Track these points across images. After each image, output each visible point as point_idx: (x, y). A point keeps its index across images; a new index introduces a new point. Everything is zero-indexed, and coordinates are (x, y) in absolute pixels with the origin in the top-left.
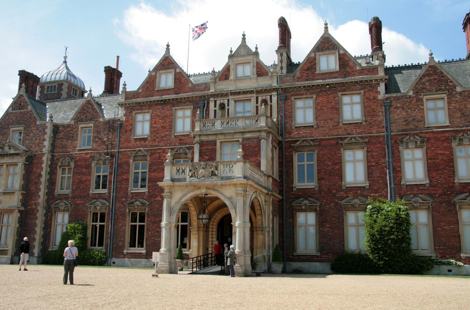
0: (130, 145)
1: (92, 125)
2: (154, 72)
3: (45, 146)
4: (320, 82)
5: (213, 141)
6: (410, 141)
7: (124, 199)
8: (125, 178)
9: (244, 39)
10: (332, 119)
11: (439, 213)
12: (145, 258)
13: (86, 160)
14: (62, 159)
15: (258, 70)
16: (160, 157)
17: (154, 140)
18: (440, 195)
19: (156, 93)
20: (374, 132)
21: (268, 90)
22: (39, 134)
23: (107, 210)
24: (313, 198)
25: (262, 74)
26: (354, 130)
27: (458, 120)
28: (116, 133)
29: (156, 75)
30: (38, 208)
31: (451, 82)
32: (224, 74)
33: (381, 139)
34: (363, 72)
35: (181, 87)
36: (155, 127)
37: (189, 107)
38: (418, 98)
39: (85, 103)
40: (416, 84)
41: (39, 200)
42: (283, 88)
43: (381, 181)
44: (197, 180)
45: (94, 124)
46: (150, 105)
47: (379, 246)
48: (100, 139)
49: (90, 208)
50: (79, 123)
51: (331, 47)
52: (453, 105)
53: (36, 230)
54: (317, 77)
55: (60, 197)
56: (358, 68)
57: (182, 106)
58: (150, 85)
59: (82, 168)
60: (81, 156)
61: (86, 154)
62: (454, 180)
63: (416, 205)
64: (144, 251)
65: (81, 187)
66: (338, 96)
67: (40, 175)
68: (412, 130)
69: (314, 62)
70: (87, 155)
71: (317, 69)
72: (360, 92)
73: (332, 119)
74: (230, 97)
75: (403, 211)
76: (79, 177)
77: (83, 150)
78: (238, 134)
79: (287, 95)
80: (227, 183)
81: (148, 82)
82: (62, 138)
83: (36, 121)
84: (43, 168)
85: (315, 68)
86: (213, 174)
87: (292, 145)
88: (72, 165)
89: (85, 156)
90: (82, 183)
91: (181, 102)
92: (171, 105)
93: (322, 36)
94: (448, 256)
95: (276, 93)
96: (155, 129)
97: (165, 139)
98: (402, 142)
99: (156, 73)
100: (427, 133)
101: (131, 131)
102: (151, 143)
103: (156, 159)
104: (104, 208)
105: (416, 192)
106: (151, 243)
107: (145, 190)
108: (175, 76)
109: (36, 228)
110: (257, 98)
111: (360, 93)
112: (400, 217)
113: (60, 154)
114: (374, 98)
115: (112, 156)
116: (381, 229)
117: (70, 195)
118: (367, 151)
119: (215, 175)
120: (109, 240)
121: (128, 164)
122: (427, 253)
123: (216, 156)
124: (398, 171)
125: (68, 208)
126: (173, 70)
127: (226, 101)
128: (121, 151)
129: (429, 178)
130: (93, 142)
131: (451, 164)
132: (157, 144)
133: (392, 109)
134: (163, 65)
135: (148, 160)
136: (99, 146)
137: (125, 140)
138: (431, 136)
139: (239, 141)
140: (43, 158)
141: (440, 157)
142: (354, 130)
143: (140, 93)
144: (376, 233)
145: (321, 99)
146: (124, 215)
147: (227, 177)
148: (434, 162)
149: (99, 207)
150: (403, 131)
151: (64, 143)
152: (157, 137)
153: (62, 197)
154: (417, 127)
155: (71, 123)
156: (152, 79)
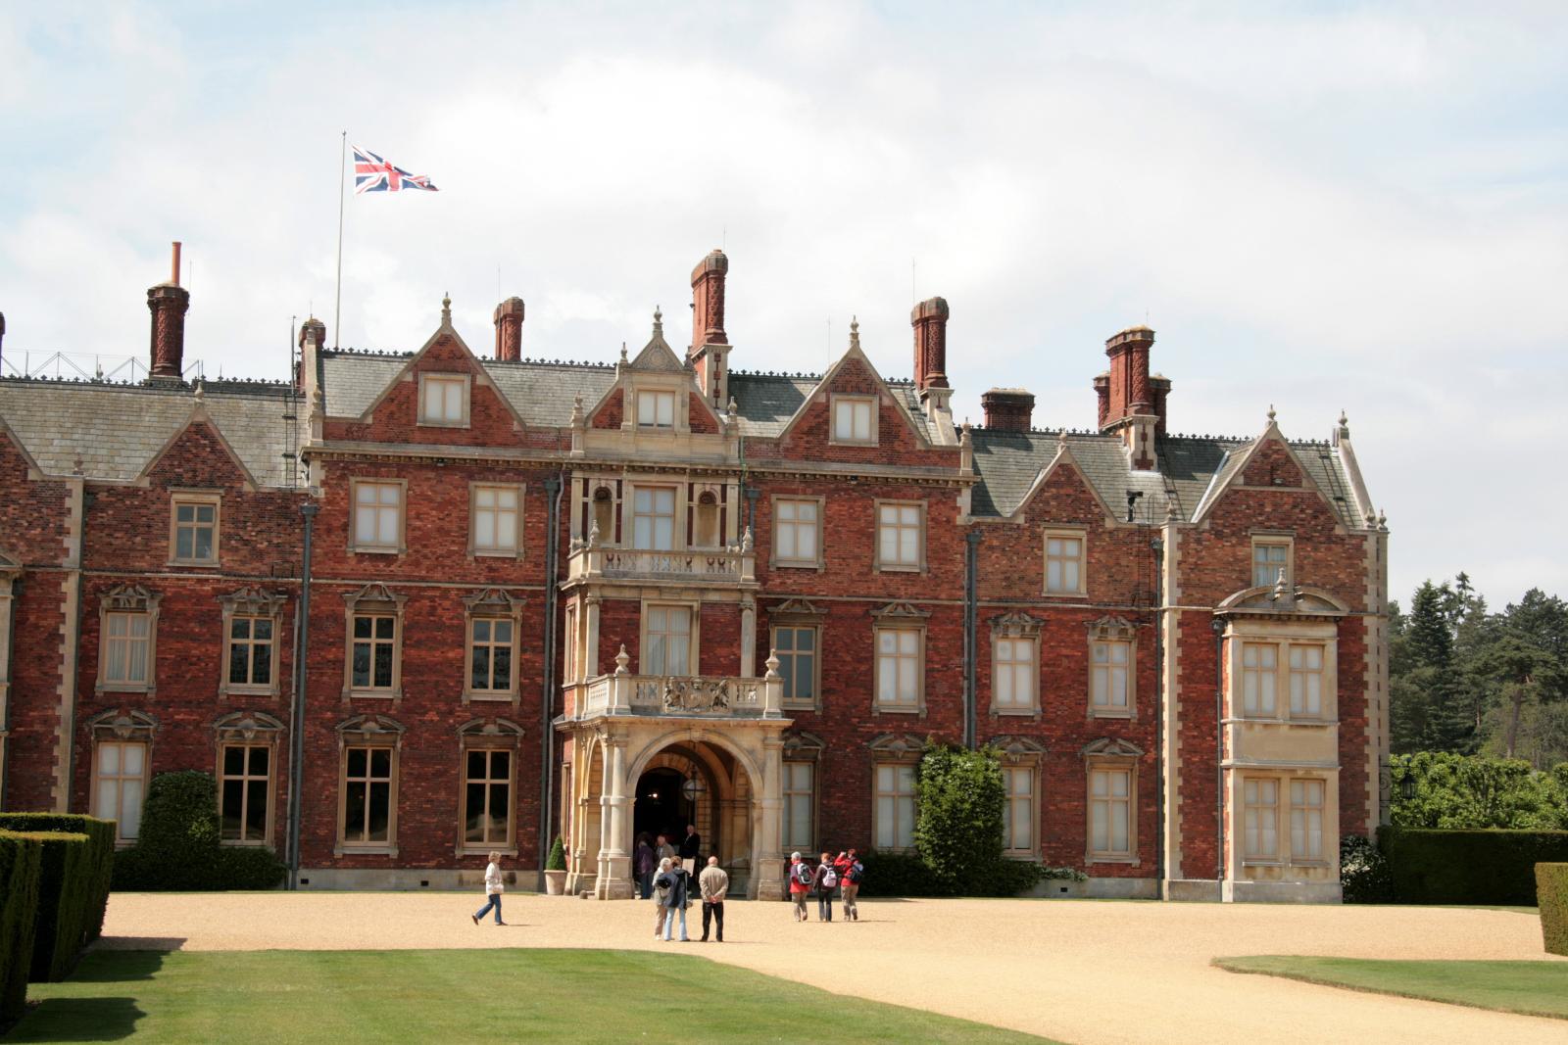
0: (345, 568)
1: (216, 499)
2: (411, 373)
3: (67, 550)
5: (630, 602)
6: (1013, 624)
7: (329, 714)
8: (331, 657)
9: (658, 326)
10: (857, 558)
11: (1053, 775)
12: (394, 868)
13: (200, 598)
14: (116, 591)
15: (693, 414)
16: (433, 610)
17: (417, 564)
18: (1060, 740)
19: (417, 435)
20: (943, 596)
21: (718, 472)
22: (40, 512)
23: (278, 741)
24: (810, 732)
25: (702, 428)
26: (903, 588)
27: (1103, 589)
28: (297, 531)
29: (416, 382)
30: (56, 733)
31: (1097, 505)
32: (608, 412)
33: (956, 614)
34: (929, 458)
35: (490, 427)
36: (419, 529)
37: (515, 485)
38: (1033, 532)
39: (188, 431)
40: (1033, 502)
41: (58, 708)
42: (753, 472)
43: (950, 705)
44: (685, 713)
45: (222, 497)
46: (401, 468)
47: (950, 843)
48: (246, 543)
49: (222, 736)
50: (170, 489)
51: (863, 386)
52: (1097, 555)
53: (53, 795)
54: (830, 454)
55: (114, 701)
56: (919, 446)
57: (494, 480)
58: (400, 409)
59: (188, 620)
60: (184, 587)
61: (199, 581)
62: (1085, 710)
63: (1013, 758)
64: (394, 853)
65: (188, 676)
66: (872, 507)
67: (56, 637)
68: (1015, 599)
69: (824, 416)
70: (202, 585)
71: (831, 435)
72: (919, 502)
73: (857, 558)
74: (625, 476)
75: (993, 771)
76: (179, 646)
77: (191, 570)
78: (692, 593)
79: (762, 489)
80: (748, 723)
81: (392, 400)
82: (109, 526)
83: (26, 469)
84: (63, 615)
85: (827, 432)
86: (718, 702)
87: (770, 609)
88: (154, 610)
89: (198, 587)
90: (191, 664)
91: (491, 470)
92: (463, 475)
93: (846, 357)
94: (1062, 862)
95: (736, 481)
96: (418, 533)
97: (448, 562)
98: (997, 624)
99: (416, 376)
100: (1045, 609)
101: (345, 527)
102: (407, 569)
103: (424, 612)
104: (267, 735)
105: (1015, 732)
106: (410, 828)
107: (391, 692)
108: (473, 395)
109: (54, 788)
110: (691, 486)
111: (920, 506)
112: (990, 784)
113: (108, 574)
114: (948, 521)
115: (291, 594)
116: (954, 806)
117: (152, 695)
118: (928, 637)
119: (723, 704)
120: (289, 821)
121: (341, 622)
122: (1026, 856)
123: (638, 637)
124: (984, 684)
125: (144, 733)
126: (467, 379)
127: (614, 485)
128: (314, 584)
129: (1041, 703)
130: (221, 548)
131: (1082, 678)
132: (423, 573)
133: (982, 550)
134: (437, 357)
135: (400, 614)
136: (243, 563)
137: (326, 554)
138: (1053, 617)
139: (691, 607)
140: (64, 584)
141: (1065, 662)
142: (903, 588)
143: (368, 426)
144: (945, 816)
145: (835, 507)
146: (330, 756)
147: (745, 710)
148: (1052, 672)
149: (250, 732)
150: (1000, 600)
151: (118, 542)
152: (425, 557)
153: (123, 700)
154: (1027, 595)
155: (141, 485)
156: (404, 392)
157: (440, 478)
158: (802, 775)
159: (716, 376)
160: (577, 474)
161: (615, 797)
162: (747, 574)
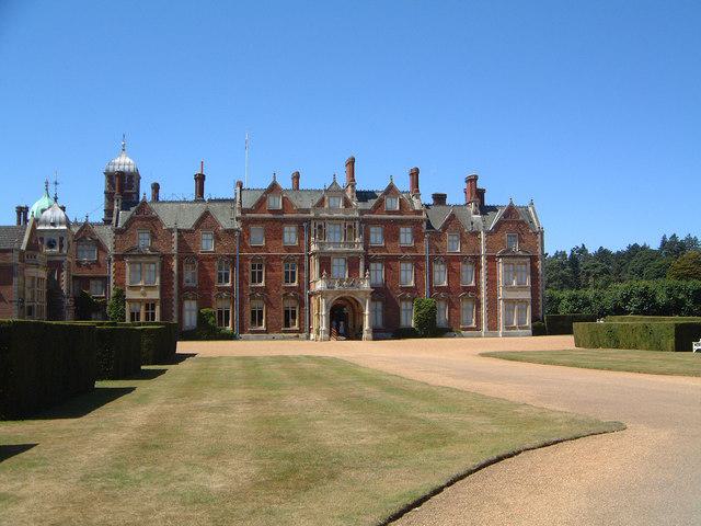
4: (386, 216)
88: (197, 264)
157: (274, 226)
158: (380, 305)
159: (353, 191)
160: (313, 222)
161: (324, 313)
162: (361, 248)
